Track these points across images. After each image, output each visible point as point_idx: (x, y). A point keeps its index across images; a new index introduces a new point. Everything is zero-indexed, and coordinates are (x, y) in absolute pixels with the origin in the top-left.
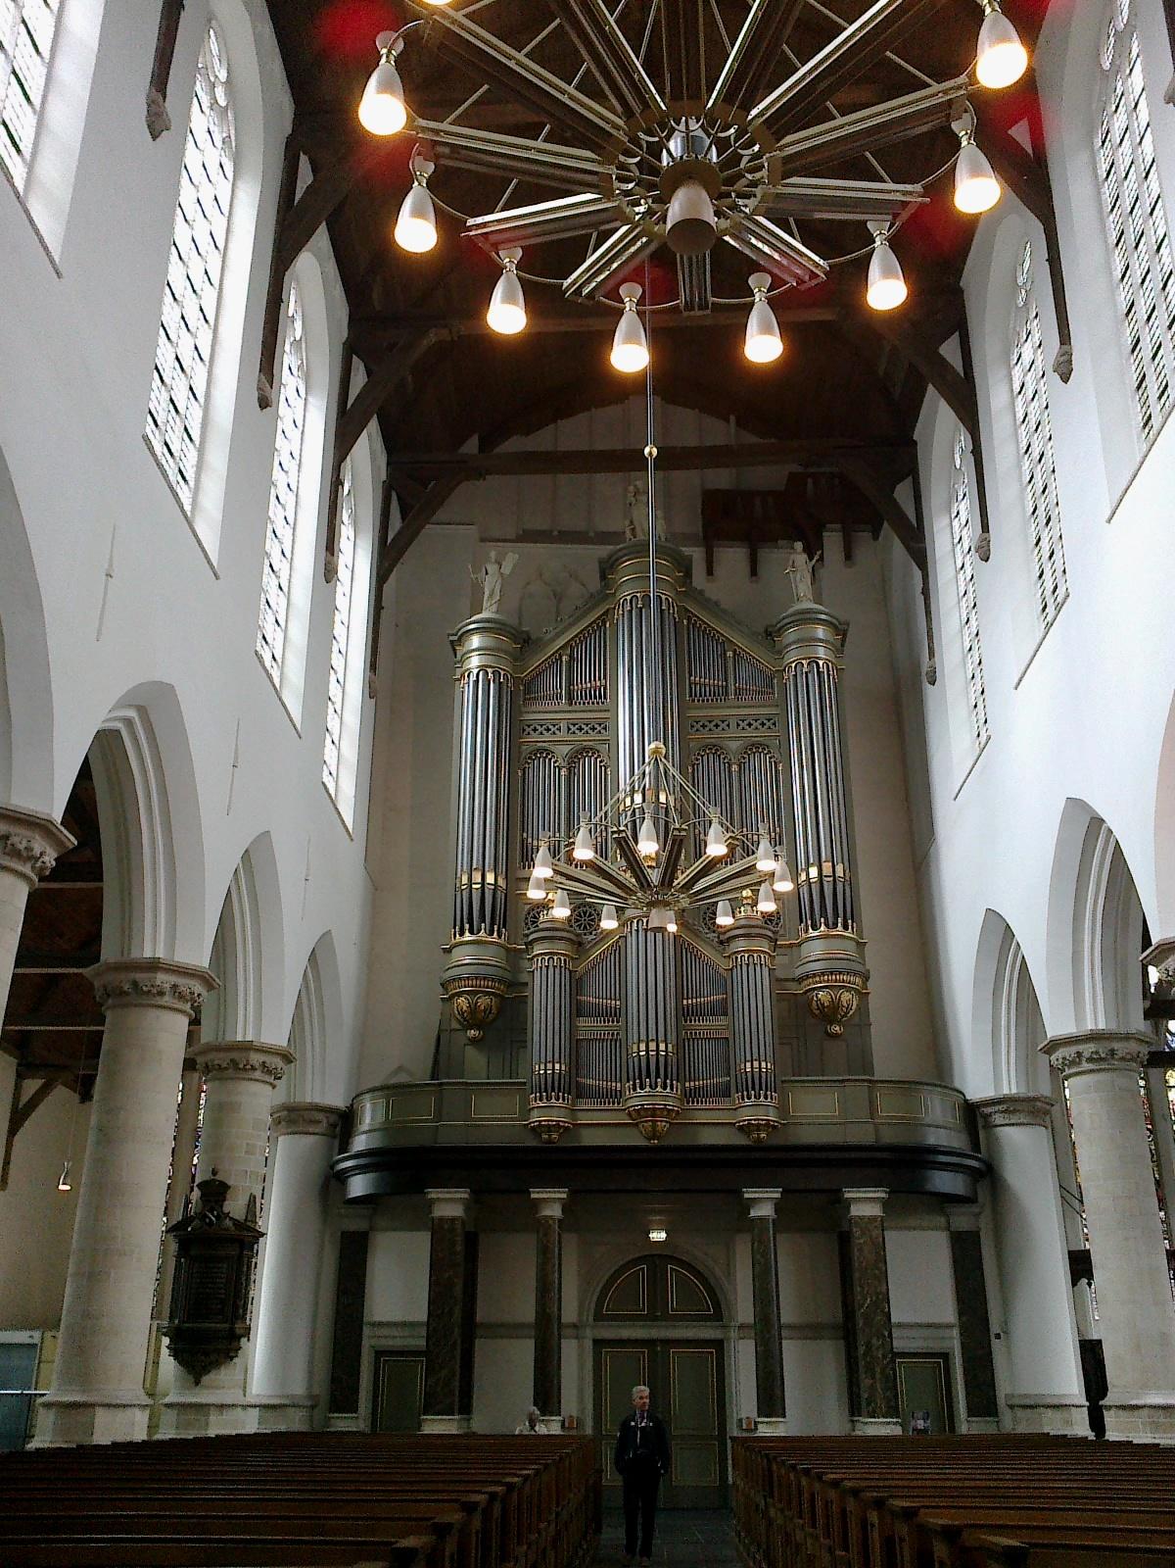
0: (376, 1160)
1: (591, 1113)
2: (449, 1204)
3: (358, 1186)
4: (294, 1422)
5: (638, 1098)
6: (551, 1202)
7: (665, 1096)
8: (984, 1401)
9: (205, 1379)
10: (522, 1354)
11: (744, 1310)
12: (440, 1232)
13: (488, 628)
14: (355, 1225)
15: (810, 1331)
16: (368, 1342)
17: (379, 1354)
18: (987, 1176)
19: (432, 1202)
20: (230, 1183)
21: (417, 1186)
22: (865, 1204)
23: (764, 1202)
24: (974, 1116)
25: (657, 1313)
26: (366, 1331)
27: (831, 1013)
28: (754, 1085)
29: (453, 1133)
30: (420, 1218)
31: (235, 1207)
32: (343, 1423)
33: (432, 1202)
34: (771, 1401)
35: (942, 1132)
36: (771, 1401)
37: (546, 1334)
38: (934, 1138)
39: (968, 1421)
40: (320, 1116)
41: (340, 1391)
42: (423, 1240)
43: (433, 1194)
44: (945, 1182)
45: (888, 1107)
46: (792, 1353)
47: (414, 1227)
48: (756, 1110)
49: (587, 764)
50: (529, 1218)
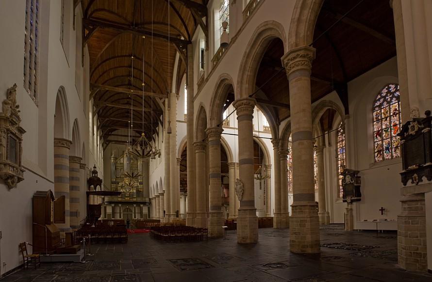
0: (107, 202)
1: (123, 199)
2: (113, 205)
3: (106, 204)
5: (126, 199)
6: (120, 205)
7: (128, 199)
8: (149, 217)
10: (119, 214)
11: (133, 212)
12: (112, 207)
13: (113, 157)
15: (138, 213)
18: (150, 203)
21: (110, 204)
22: (142, 205)
23: (135, 205)
24: (150, 199)
25: (128, 212)
27: (141, 191)
28: (134, 198)
29: (113, 201)
30: (111, 206)
34: (135, 217)
35: (147, 200)
36: (135, 217)
37: (120, 213)
38: (147, 201)
39: (159, 218)
41: (105, 217)
42: (111, 207)
44: (147, 204)
45: (144, 200)
46: (136, 214)
48: (135, 200)
49: (122, 170)
50: (118, 206)
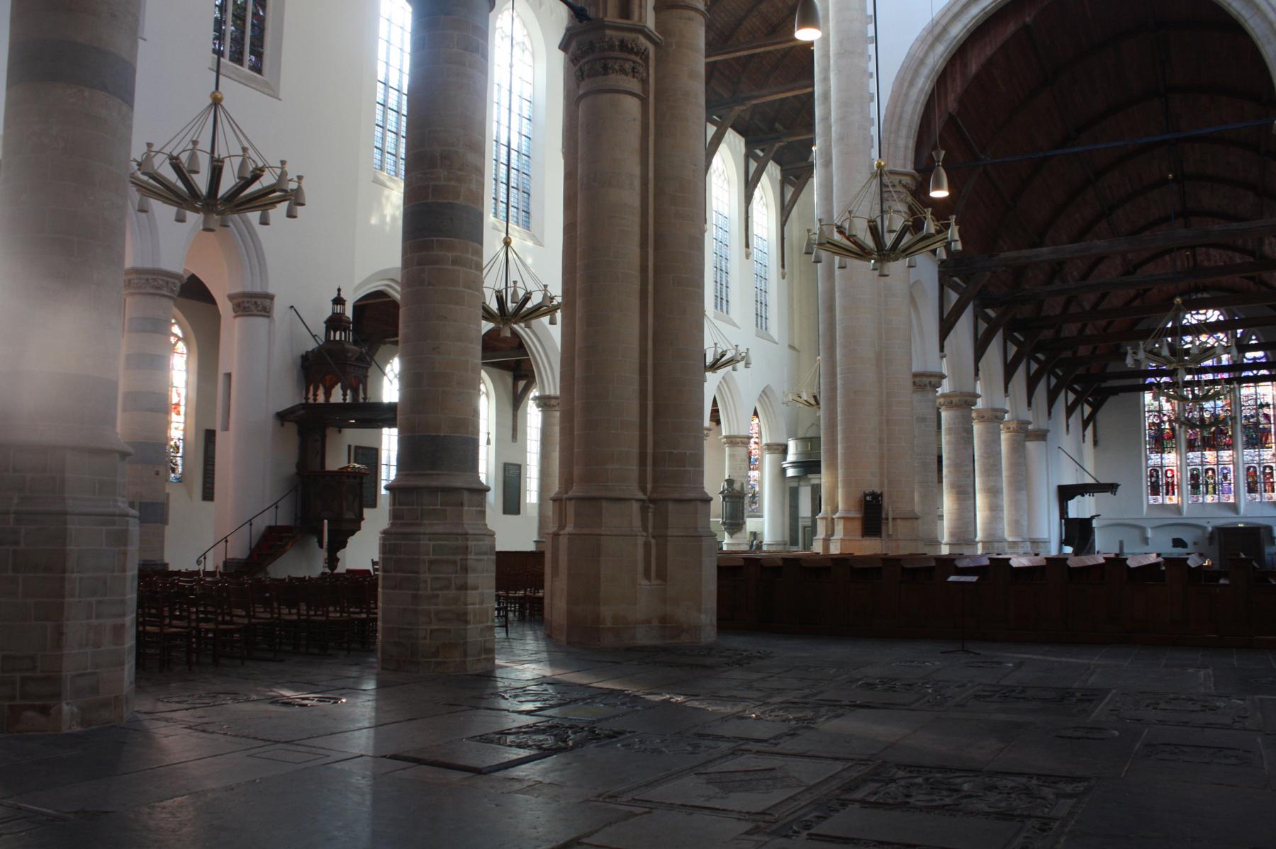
0: (796, 465)
3: (791, 473)
4: (779, 548)
9: (734, 536)
14: (794, 484)
16: (801, 524)
17: (805, 527)
19: (810, 479)
20: (735, 479)
26: (800, 520)
31: (737, 486)
32: (794, 548)
33: (810, 479)
40: (779, 447)
41: (794, 541)
43: (810, 476)
47: (807, 486)
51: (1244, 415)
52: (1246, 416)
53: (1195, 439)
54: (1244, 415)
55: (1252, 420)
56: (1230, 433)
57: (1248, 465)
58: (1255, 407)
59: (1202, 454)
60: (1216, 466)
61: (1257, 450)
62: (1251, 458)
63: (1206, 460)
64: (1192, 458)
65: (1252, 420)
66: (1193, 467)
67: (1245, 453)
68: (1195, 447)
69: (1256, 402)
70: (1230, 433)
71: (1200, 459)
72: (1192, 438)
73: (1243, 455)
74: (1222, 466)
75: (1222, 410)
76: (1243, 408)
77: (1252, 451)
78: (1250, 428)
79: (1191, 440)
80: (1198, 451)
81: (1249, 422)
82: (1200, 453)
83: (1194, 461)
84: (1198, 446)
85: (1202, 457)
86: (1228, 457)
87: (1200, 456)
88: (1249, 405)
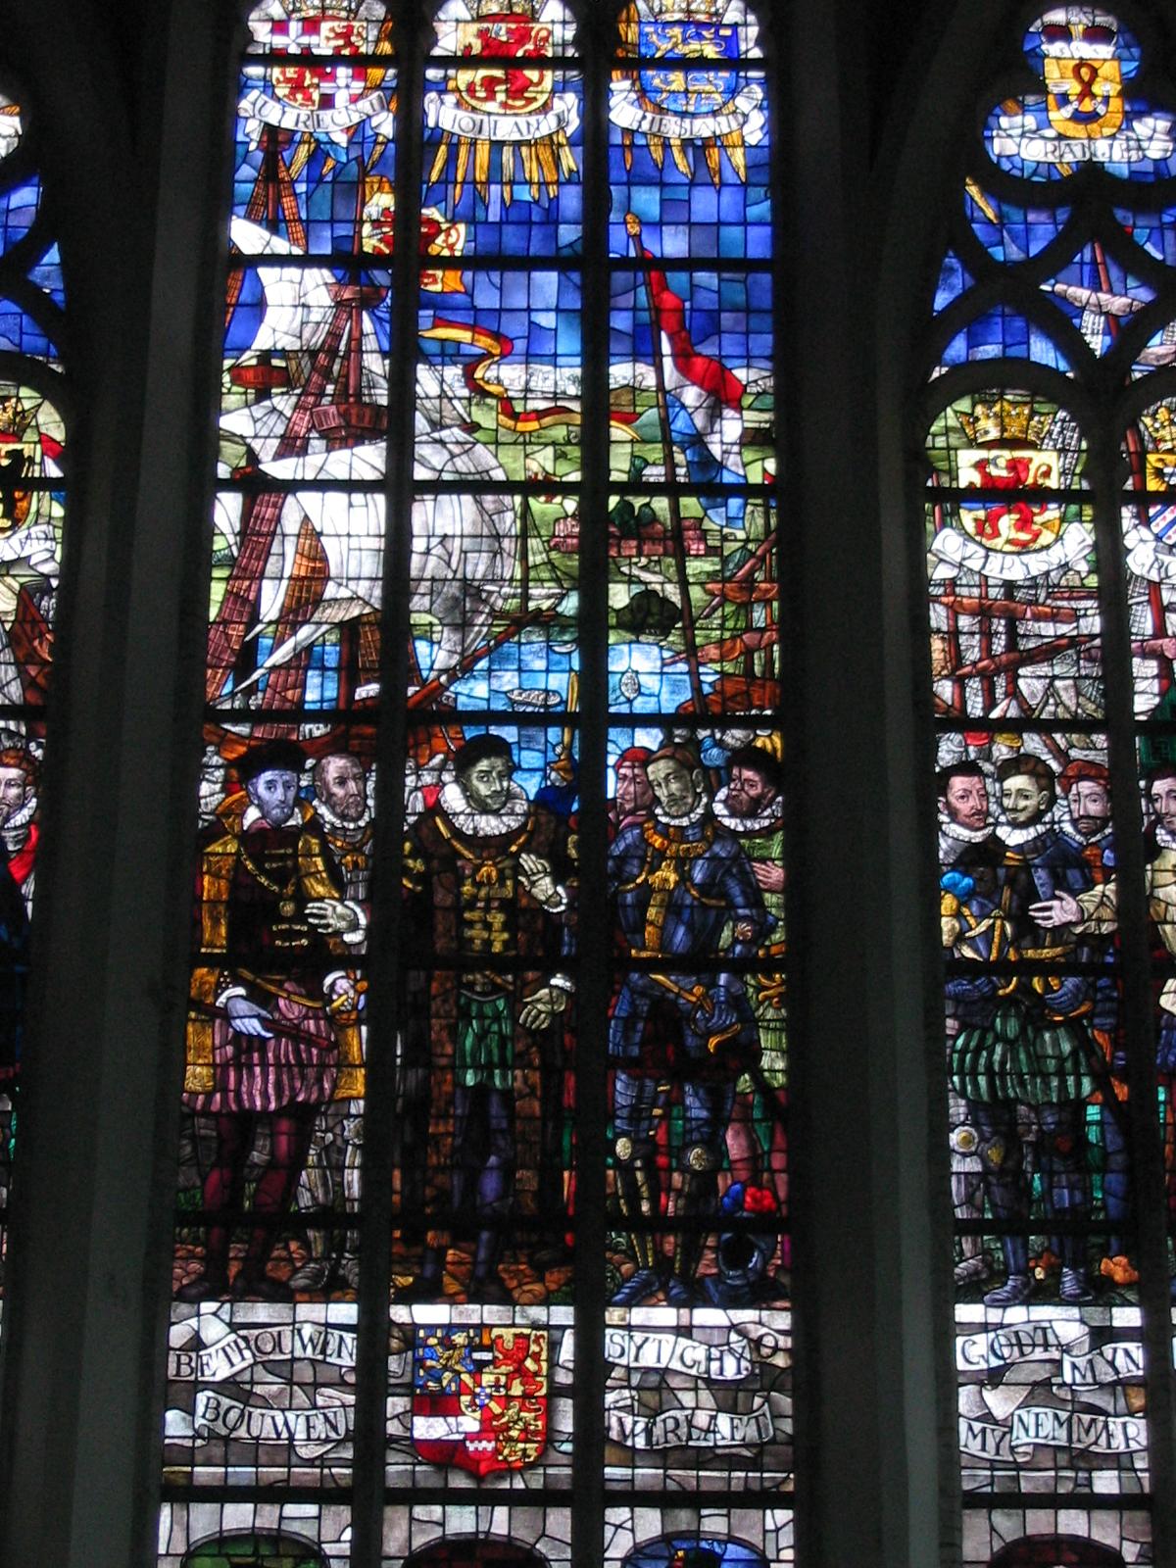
51: (954, 834)
52: (984, 855)
53: (301, 1117)
54: (954, 834)
55: (1061, 911)
56: (773, 1062)
57: (1007, 1525)
58: (1097, 748)
59: (373, 1333)
60: (560, 1521)
61: (1128, 1317)
62: (1041, 1426)
63: (429, 1428)
64: (234, 1388)
65: (1061, 911)
66: (238, 1516)
67: (973, 1353)
68: (299, 1224)
69: (1117, 685)
70: (773, 1062)
71: (340, 1402)
72: (260, 1092)
73: (947, 1381)
74: (650, 1523)
75: (686, 757)
76: (949, 749)
77: (1067, 1324)
78: (1035, 1013)
79: (246, 1123)
80: (327, 1290)
81: (1027, 930)
82: (346, 1312)
83: (264, 1424)
84: (331, 1216)
85: (371, 1385)
86: (730, 1396)
87: (346, 1354)
88: (1027, 722)
